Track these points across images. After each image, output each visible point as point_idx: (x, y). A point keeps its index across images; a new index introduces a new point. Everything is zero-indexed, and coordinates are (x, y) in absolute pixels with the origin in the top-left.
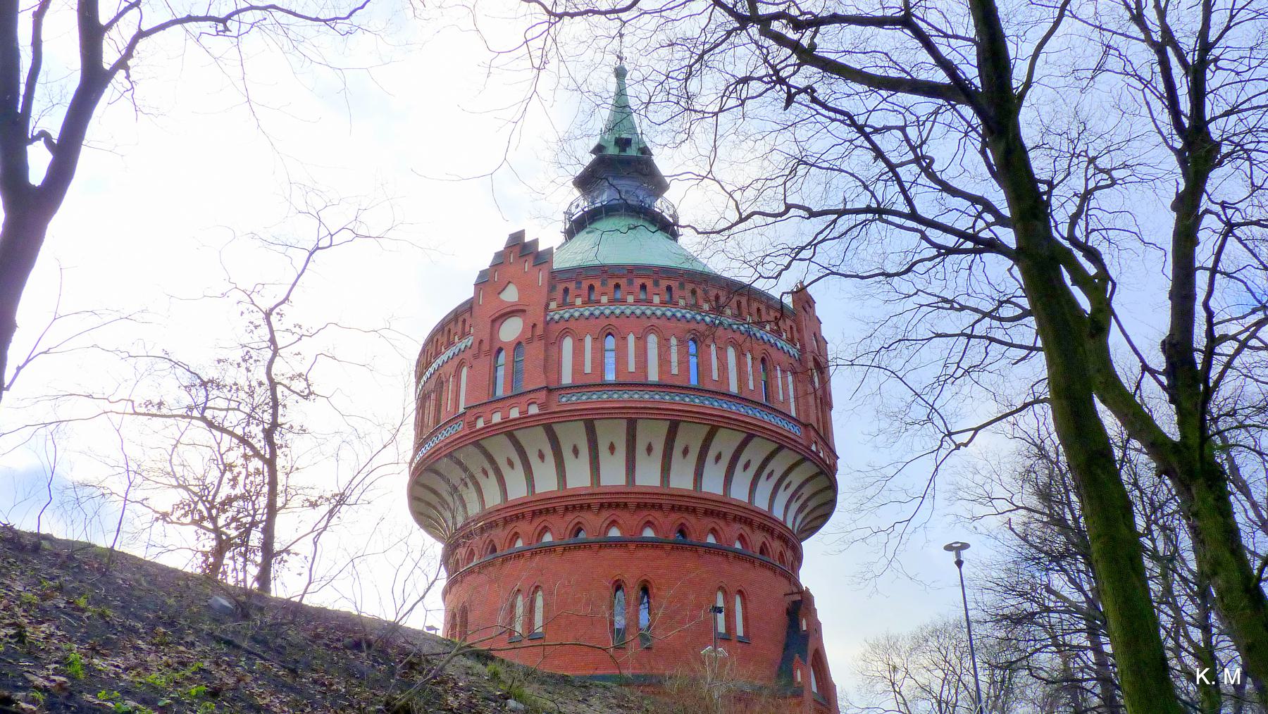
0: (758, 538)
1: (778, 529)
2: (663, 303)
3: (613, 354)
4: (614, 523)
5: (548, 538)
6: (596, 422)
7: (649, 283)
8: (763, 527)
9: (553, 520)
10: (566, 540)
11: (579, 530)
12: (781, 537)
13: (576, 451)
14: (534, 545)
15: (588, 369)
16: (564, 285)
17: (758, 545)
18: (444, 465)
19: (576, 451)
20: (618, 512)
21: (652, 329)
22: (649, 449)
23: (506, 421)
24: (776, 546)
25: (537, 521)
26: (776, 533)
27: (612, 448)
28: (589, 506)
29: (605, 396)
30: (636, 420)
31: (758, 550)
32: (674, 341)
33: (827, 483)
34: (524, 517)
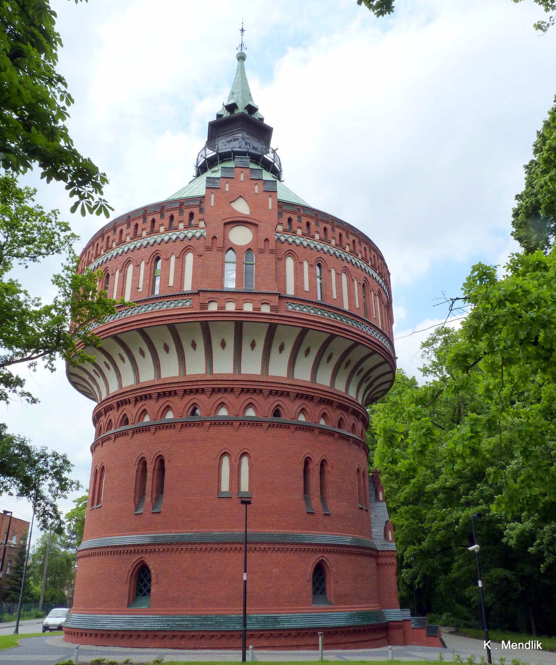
2: (304, 235)
3: (233, 266)
4: (250, 405)
5: (170, 415)
7: (295, 218)
9: (174, 401)
10: (184, 419)
11: (195, 409)
14: (158, 422)
20: (226, 395)
21: (290, 253)
23: (239, 312)
25: (162, 401)
27: (223, 345)
30: (242, 322)
32: (306, 264)
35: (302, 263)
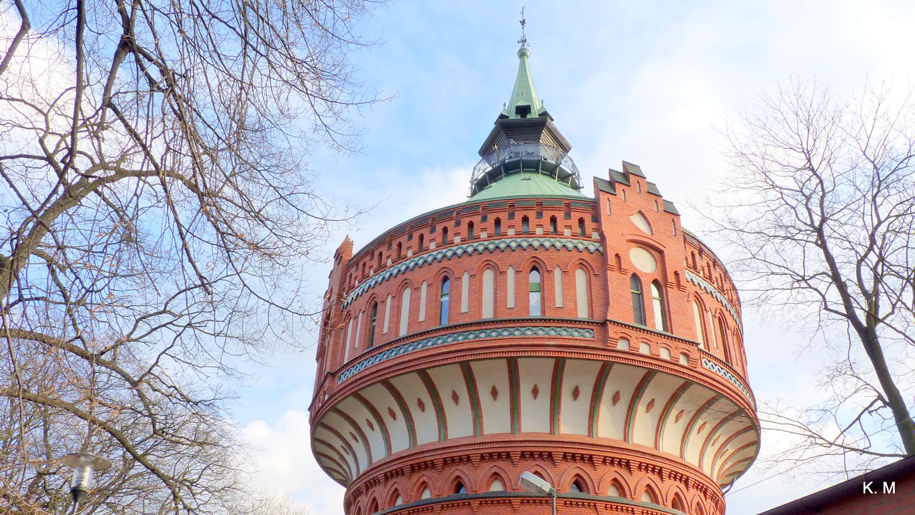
0: (669, 488)
1: (693, 477)
6: (519, 360)
8: (675, 476)
12: (699, 487)
13: (455, 398)
15: (511, 303)
16: (467, 220)
17: (671, 496)
18: (334, 420)
19: (455, 398)
22: (535, 392)
24: (692, 496)
26: (691, 483)
28: (469, 458)
29: (482, 335)
31: (669, 503)
33: (746, 422)
34: (403, 473)
35: (503, 273)
